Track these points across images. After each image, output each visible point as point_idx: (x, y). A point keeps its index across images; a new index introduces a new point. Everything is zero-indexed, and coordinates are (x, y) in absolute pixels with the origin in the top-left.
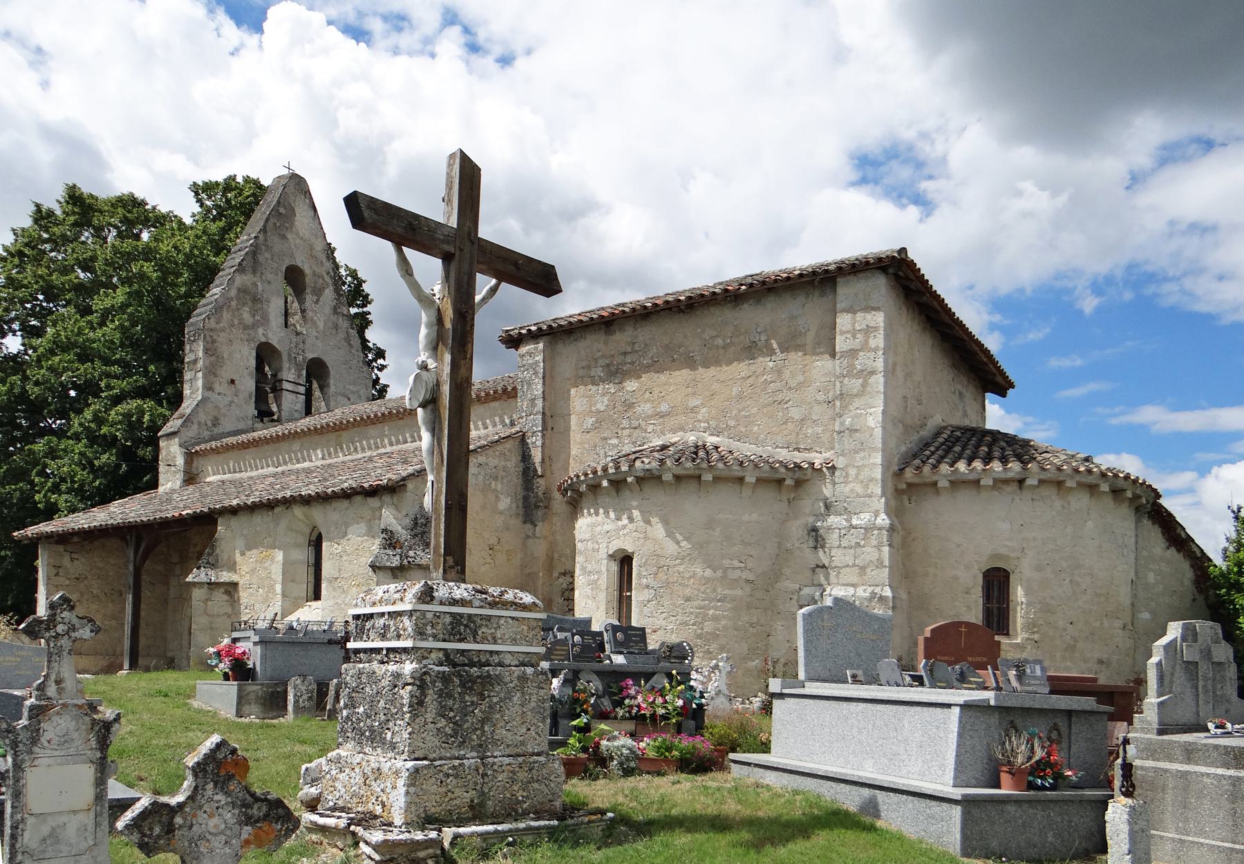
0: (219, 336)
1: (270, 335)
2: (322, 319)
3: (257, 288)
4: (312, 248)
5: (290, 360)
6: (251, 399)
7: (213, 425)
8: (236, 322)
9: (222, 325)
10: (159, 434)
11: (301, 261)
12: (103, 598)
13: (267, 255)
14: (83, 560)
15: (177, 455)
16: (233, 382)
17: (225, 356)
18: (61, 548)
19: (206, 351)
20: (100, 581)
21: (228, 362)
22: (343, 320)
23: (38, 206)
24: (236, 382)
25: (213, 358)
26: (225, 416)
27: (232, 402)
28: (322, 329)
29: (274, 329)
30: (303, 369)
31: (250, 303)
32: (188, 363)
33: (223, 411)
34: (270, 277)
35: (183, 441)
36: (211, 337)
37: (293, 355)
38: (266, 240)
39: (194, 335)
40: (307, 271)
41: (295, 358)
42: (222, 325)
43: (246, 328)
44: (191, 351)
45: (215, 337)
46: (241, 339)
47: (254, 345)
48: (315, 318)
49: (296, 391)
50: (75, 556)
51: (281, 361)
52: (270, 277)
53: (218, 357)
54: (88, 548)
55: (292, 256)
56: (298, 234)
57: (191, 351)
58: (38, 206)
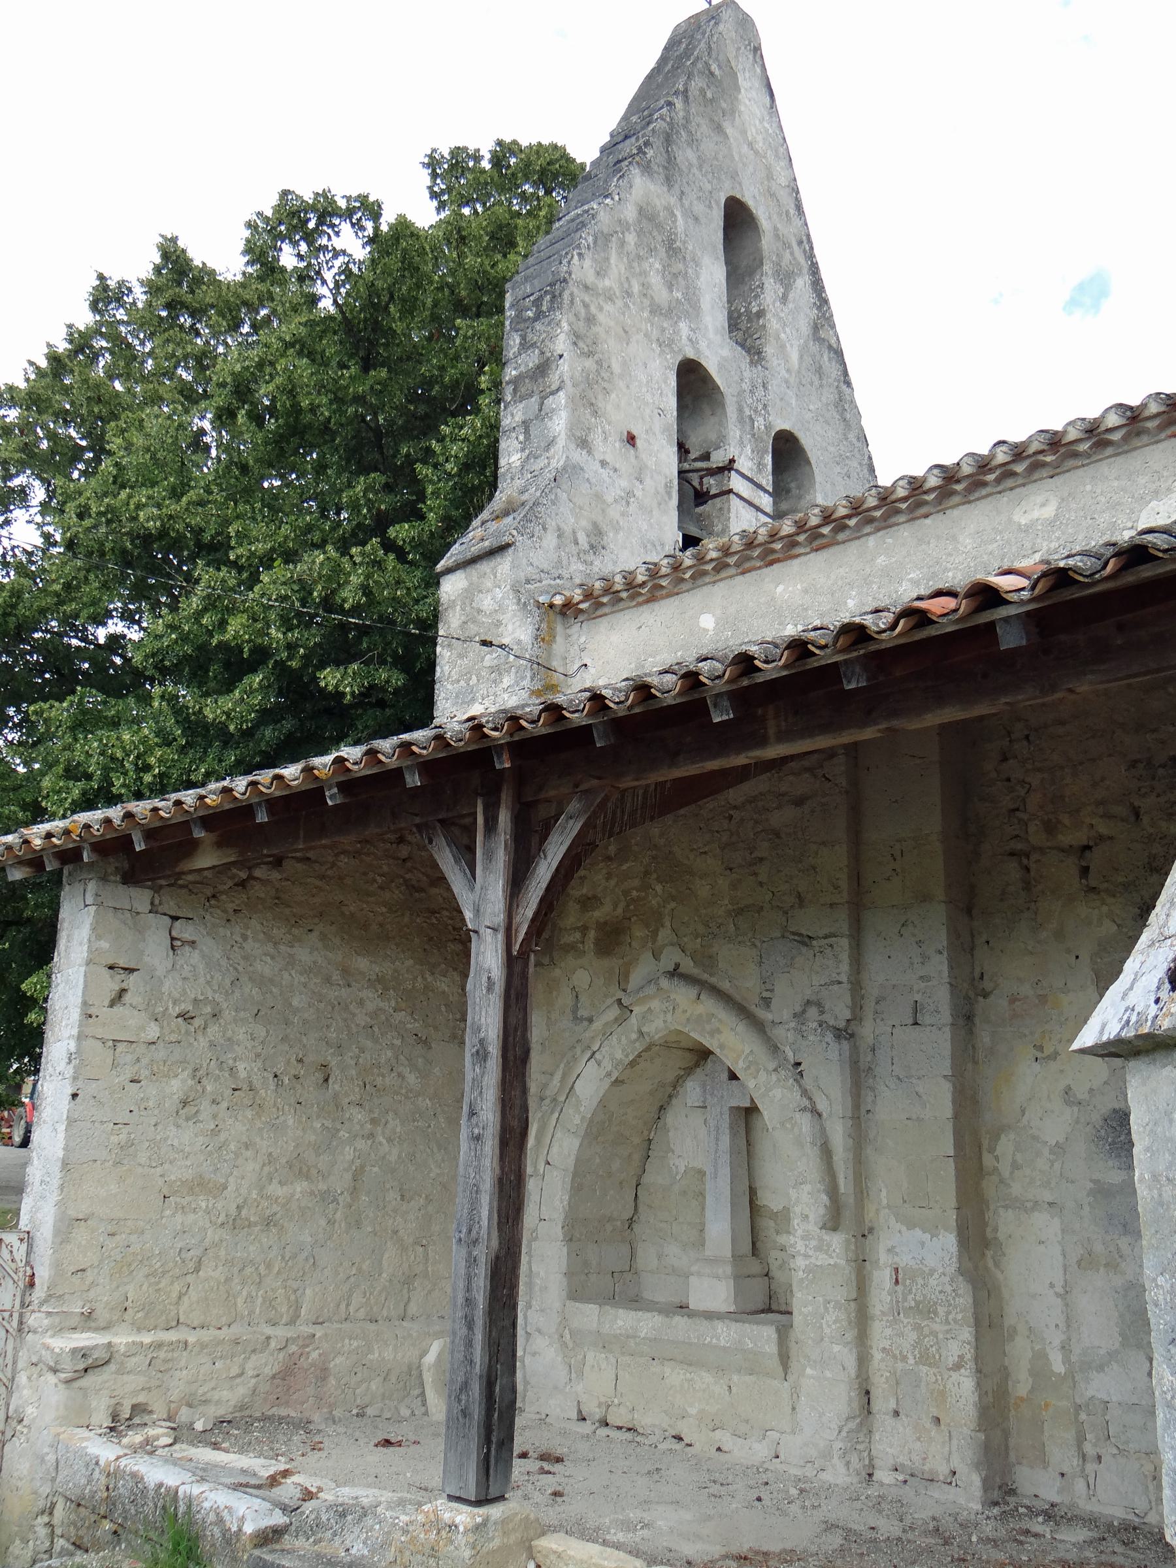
0: (601, 309)
1: (703, 345)
2: (796, 343)
3: (674, 222)
4: (770, 177)
5: (741, 420)
6: (670, 498)
7: (592, 547)
8: (636, 288)
9: (607, 283)
10: (440, 567)
11: (751, 197)
12: (267, 1093)
13: (690, 154)
14: (208, 945)
15: (505, 618)
16: (631, 439)
17: (616, 367)
18: (141, 898)
19: (576, 338)
20: (261, 1032)
21: (621, 384)
22: (830, 359)
23: (101, 277)
24: (639, 442)
25: (589, 363)
26: (617, 528)
27: (630, 494)
28: (797, 367)
29: (711, 335)
30: (767, 451)
31: (662, 252)
32: (516, 381)
33: (614, 512)
34: (699, 208)
35: (522, 576)
36: (586, 306)
37: (747, 412)
38: (687, 119)
39: (537, 303)
40: (764, 222)
41: (752, 421)
42: (607, 283)
43: (655, 310)
44: (525, 346)
45: (593, 309)
46: (646, 335)
47: (674, 361)
48: (783, 336)
49: (756, 502)
50: (184, 931)
51: (722, 424)
52: (699, 208)
53: (599, 363)
54: (230, 907)
55: (734, 176)
56: (744, 132)
57: (525, 346)
58: (101, 277)
